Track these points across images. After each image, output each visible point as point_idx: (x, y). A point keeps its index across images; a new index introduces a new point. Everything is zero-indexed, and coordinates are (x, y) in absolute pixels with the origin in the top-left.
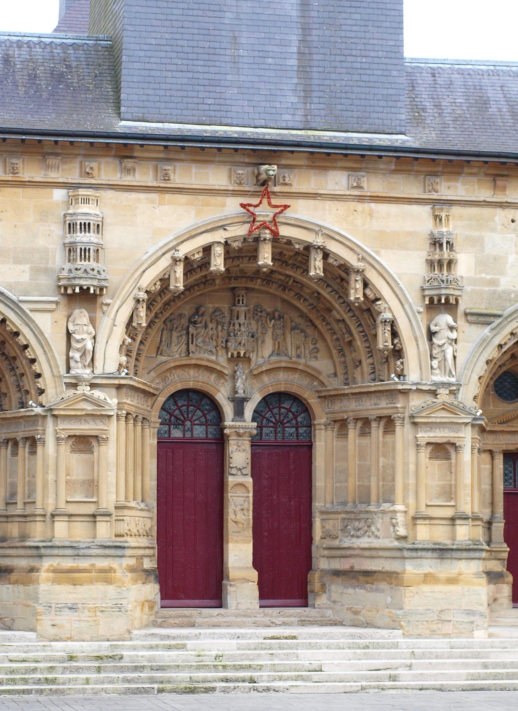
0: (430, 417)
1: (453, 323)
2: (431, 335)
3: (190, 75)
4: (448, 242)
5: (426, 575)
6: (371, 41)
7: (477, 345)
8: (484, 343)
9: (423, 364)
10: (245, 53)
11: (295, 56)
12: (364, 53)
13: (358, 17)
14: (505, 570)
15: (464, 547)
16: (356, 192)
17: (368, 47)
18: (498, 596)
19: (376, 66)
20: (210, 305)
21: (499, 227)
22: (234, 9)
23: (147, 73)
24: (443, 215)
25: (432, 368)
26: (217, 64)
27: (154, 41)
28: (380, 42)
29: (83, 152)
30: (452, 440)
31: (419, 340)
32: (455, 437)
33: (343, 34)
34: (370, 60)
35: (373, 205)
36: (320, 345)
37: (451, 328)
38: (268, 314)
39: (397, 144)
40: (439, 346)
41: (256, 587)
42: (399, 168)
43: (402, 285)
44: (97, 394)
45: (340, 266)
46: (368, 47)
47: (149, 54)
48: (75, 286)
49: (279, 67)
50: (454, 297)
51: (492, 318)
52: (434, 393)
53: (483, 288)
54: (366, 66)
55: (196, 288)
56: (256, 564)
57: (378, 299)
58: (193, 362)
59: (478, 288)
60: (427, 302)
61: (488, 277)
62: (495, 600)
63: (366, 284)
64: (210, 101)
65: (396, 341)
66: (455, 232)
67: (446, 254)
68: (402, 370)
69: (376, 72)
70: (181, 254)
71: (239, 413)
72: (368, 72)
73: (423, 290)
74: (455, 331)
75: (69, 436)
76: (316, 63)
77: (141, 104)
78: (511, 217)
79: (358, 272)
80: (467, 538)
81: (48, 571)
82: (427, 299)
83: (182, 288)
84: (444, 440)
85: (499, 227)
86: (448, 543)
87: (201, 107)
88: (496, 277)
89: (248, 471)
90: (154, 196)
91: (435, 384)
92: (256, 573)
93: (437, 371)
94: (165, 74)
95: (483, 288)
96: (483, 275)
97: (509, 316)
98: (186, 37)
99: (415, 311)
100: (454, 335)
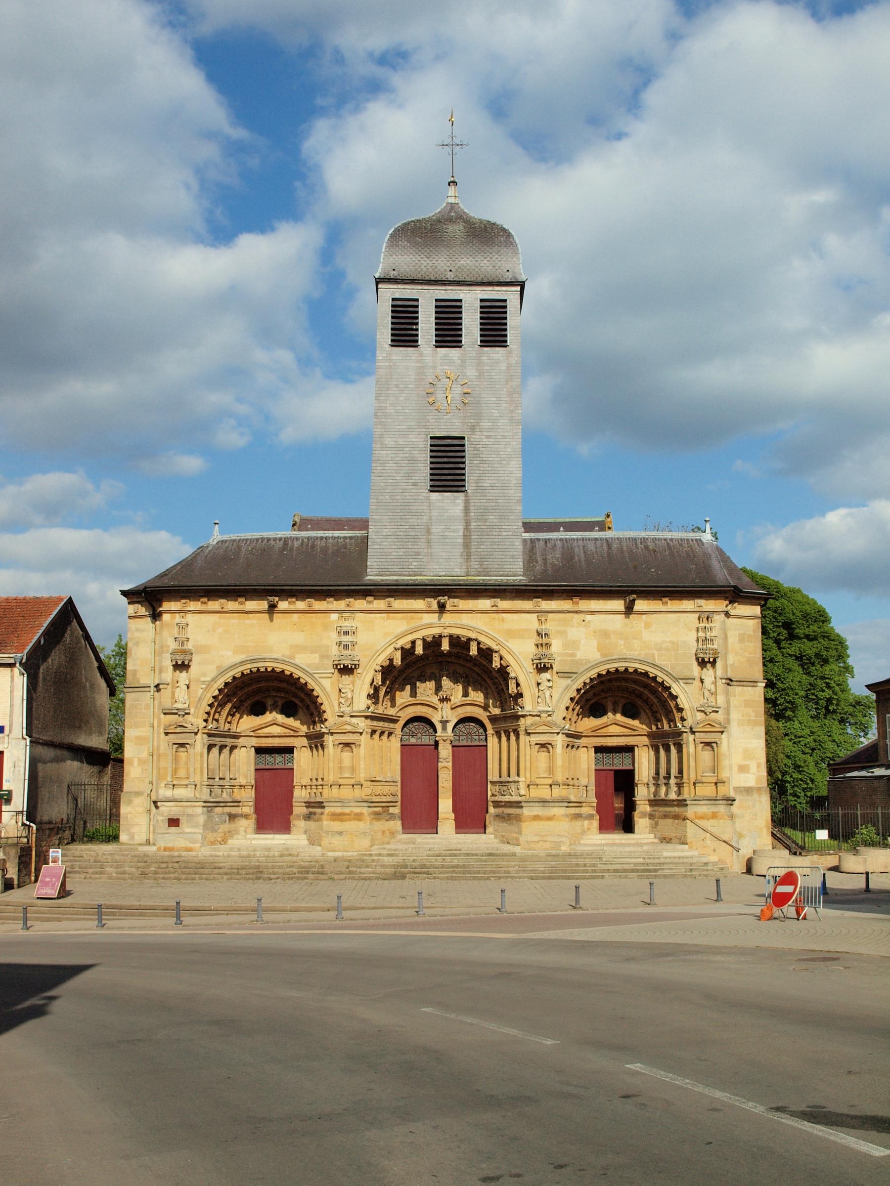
1: (549, 678)
2: (538, 684)
3: (404, 550)
5: (535, 816)
6: (504, 527)
8: (567, 688)
10: (435, 537)
11: (462, 537)
12: (499, 533)
13: (496, 514)
14: (595, 812)
16: (495, 608)
17: (502, 530)
19: (506, 540)
20: (429, 671)
21: (576, 625)
22: (428, 514)
23: (381, 550)
24: (543, 619)
26: (419, 544)
27: (385, 534)
28: (509, 527)
29: (345, 594)
30: (550, 742)
33: (488, 524)
34: (503, 537)
35: (504, 615)
36: (489, 691)
37: (549, 681)
38: (460, 675)
39: (516, 583)
41: (454, 822)
43: (520, 658)
44: (354, 720)
45: (487, 648)
46: (502, 530)
47: (382, 540)
48: (340, 664)
49: (452, 544)
52: (539, 716)
54: (501, 540)
55: (418, 662)
56: (455, 810)
57: (508, 666)
58: (419, 702)
60: (535, 667)
61: (570, 652)
63: (501, 658)
64: (415, 564)
67: (545, 640)
69: (506, 543)
70: (398, 646)
71: (444, 728)
72: (502, 543)
73: (533, 660)
74: (551, 682)
75: (340, 744)
76: (474, 540)
77: (378, 567)
78: (582, 619)
79: (496, 652)
81: (328, 814)
83: (400, 663)
85: (576, 625)
86: (548, 798)
87: (410, 567)
89: (450, 759)
90: (384, 615)
91: (539, 712)
92: (453, 815)
93: (540, 704)
94: (390, 550)
96: (567, 651)
98: (402, 530)
100: (550, 684)
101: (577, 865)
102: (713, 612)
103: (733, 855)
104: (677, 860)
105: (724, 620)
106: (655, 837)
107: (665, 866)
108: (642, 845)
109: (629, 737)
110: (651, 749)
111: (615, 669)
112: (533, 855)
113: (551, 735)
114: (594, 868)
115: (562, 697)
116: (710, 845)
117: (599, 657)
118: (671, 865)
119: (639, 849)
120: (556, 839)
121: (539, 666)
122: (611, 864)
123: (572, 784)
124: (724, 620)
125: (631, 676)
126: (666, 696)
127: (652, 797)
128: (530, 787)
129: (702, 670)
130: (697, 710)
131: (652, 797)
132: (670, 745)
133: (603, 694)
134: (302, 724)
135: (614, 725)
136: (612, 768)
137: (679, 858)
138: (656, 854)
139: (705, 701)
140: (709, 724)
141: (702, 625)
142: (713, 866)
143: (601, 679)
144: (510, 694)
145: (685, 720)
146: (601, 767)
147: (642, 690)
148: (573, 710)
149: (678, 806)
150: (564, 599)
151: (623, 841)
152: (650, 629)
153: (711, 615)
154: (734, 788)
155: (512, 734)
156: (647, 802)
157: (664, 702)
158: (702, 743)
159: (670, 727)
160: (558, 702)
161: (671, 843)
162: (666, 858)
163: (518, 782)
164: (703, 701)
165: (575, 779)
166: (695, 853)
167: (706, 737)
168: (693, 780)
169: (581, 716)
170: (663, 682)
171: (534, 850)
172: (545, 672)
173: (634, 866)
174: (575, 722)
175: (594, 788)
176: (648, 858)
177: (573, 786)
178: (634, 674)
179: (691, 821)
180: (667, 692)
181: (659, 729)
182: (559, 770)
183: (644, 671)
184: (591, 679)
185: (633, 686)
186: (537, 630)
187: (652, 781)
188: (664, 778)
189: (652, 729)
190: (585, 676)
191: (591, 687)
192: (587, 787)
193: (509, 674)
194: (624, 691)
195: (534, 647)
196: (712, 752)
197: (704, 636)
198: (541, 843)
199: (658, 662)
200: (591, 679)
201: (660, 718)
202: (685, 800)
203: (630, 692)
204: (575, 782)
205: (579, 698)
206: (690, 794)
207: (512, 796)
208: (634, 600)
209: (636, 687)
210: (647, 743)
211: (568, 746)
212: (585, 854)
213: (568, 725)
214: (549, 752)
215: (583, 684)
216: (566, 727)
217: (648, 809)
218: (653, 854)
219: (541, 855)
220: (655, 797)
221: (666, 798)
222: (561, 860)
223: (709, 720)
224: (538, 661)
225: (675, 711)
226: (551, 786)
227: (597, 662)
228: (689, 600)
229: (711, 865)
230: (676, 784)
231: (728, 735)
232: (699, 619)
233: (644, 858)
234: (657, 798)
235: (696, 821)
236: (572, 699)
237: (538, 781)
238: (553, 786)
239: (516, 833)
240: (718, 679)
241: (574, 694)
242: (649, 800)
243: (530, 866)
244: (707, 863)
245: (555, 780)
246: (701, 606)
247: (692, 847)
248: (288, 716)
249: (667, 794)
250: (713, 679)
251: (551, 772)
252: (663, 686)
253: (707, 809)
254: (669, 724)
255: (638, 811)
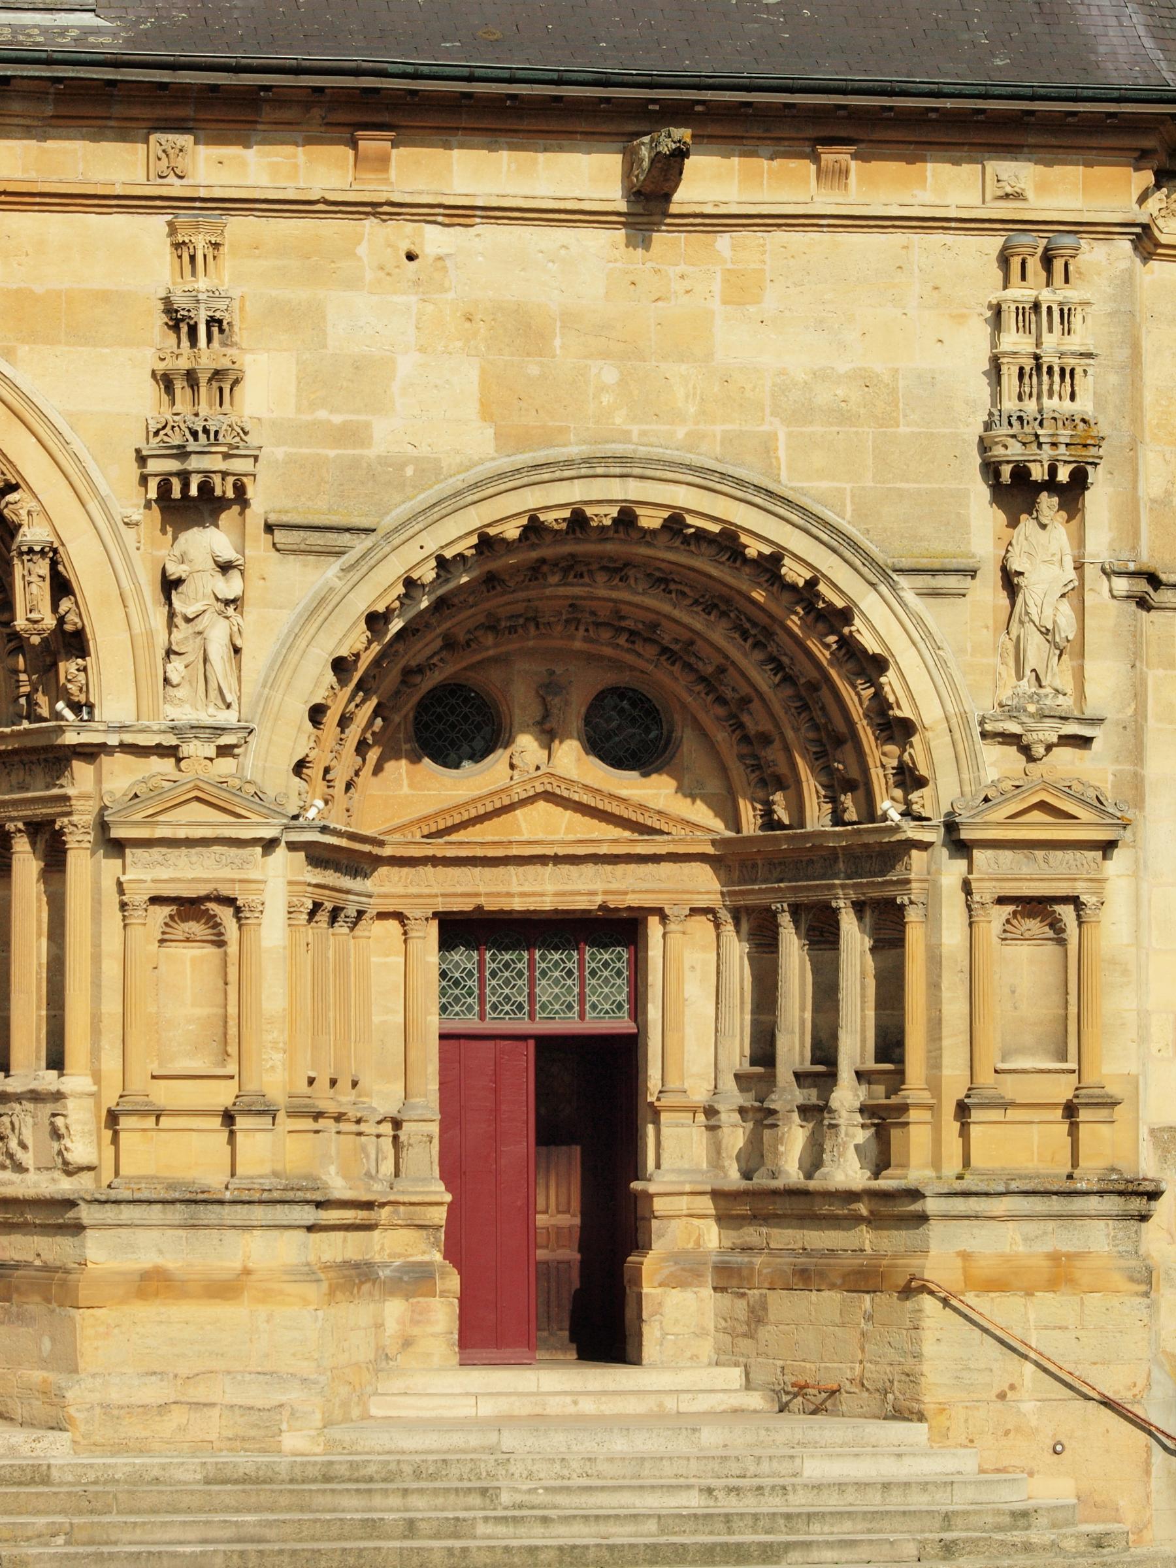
0: (157, 823)
1: (228, 553)
2: (169, 585)
4: (212, 322)
7: (300, 615)
9: (142, 670)
14: (438, 1257)
15: (256, 1196)
18: (416, 1331)
24: (200, 242)
25: (166, 680)
30: (225, 891)
31: (130, 603)
32: (233, 881)
37: (225, 568)
39: (66, 43)
40: (188, 620)
42: (64, 111)
43: (77, 445)
50: (230, 480)
51: (347, 536)
53: (321, 451)
57: (14, 488)
59: (305, 451)
60: (153, 494)
61: (337, 419)
62: (407, 1343)
65: (65, 605)
66: (235, 293)
67: (208, 357)
68: (85, 689)
73: (142, 459)
74: (235, 574)
78: (404, 246)
80: (266, 1169)
82: (153, 484)
84: (202, 890)
85: (369, 275)
86: (214, 1179)
88: (362, 418)
93: (179, 693)
95: (321, 451)
96: (322, 414)
97: (396, 530)
99: (118, 519)
100: (231, 586)
101: (372, 1527)
102: (1078, 228)
103: (1148, 1472)
104: (874, 1501)
105: (1130, 273)
106: (749, 1385)
107: (817, 1531)
108: (690, 1423)
109: (621, 868)
110: (729, 929)
111: (567, 513)
112: (137, 1480)
113: (233, 851)
114: (458, 1544)
115: (294, 658)
116: (1034, 1423)
117: (490, 449)
118: (847, 1525)
119: (681, 1445)
120: (256, 1395)
121: (176, 493)
122: (545, 1520)
123: (331, 1107)
124: (1130, 273)
125: (643, 551)
126: (823, 656)
127: (733, 1178)
128: (124, 1122)
129: (1013, 523)
130: (984, 735)
131: (733, 1178)
132: (835, 912)
133: (490, 640)
134: (688, 791)
135: (541, 805)
136: (523, 1025)
137: (886, 1486)
138: (765, 1467)
139: (1027, 686)
140: (1042, 806)
141: (1021, 293)
142: (1054, 1526)
143: (494, 565)
144: (15, 636)
145: (921, 782)
146: (470, 1023)
147: (698, 624)
148: (344, 722)
149: (875, 1221)
150: (309, 141)
151: (588, 1406)
152: (752, 309)
153: (1068, 240)
154: (1152, 1131)
155: (21, 846)
156: (706, 1205)
157: (813, 687)
158: (1001, 901)
159: (837, 820)
160: (270, 682)
161: (835, 1413)
162: (818, 1487)
163: (58, 1096)
164: (1010, 688)
165: (344, 1083)
166: (964, 1463)
167: (1026, 870)
168: (954, 1087)
169: (373, 755)
170: (812, 583)
171: (141, 1452)
172: (201, 524)
173: (662, 1532)
174: (349, 786)
175: (434, 1128)
176: (730, 1490)
177: (339, 1118)
178: (663, 539)
179: (945, 1302)
180: (832, 639)
181: (781, 826)
182: (275, 1035)
183: (715, 528)
184: (441, 562)
185: (648, 601)
186: (167, 301)
187: (733, 1096)
188: (800, 1077)
189: (734, 823)
190: (414, 544)
191: (440, 604)
192: (397, 1124)
193: (12, 529)
194: (598, 625)
195: (151, 391)
196: (1051, 948)
197: (1032, 349)
198: (178, 1416)
199: (787, 483)
200: (441, 562)
201: (783, 769)
202: (915, 1194)
203: (633, 634)
204: (345, 1099)
205: (377, 662)
206: (936, 1163)
207: (20, 1168)
208: (680, 154)
209: (666, 608)
210: (713, 900)
211: (317, 906)
212: (407, 1469)
213: (320, 803)
214: (221, 944)
215: (401, 590)
216: (312, 813)
217: (712, 1237)
218: (752, 1469)
219: (180, 1475)
220: (747, 1175)
221: (813, 1185)
222: (283, 1501)
223: (1046, 786)
224: (173, 465)
225: (867, 735)
226: (228, 1118)
227: (472, 476)
228: (956, 162)
229: (1043, 1521)
230: (862, 1110)
231: (1137, 861)
232: (1004, 260)
233: (710, 1491)
234: (761, 1181)
235: (970, 1298)
236: (341, 666)
237: (163, 1095)
238: (241, 1122)
239: (43, 1363)
240: (1091, 572)
241: (360, 635)
242: (716, 1194)
243: (126, 1537)
244: (1025, 1514)
245: (251, 1086)
246: (1018, 196)
247: (945, 1434)
248: (617, 760)
249: (814, 1162)
250: (1072, 574)
251: (233, 1049)
252: (810, 608)
253: (1026, 1239)
254: (833, 800)
255: (659, 1247)
